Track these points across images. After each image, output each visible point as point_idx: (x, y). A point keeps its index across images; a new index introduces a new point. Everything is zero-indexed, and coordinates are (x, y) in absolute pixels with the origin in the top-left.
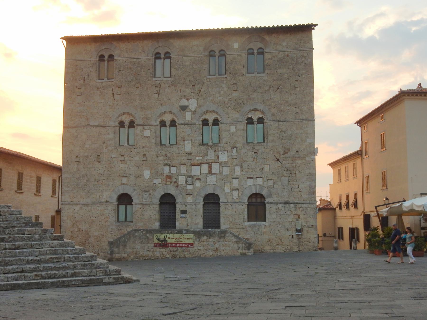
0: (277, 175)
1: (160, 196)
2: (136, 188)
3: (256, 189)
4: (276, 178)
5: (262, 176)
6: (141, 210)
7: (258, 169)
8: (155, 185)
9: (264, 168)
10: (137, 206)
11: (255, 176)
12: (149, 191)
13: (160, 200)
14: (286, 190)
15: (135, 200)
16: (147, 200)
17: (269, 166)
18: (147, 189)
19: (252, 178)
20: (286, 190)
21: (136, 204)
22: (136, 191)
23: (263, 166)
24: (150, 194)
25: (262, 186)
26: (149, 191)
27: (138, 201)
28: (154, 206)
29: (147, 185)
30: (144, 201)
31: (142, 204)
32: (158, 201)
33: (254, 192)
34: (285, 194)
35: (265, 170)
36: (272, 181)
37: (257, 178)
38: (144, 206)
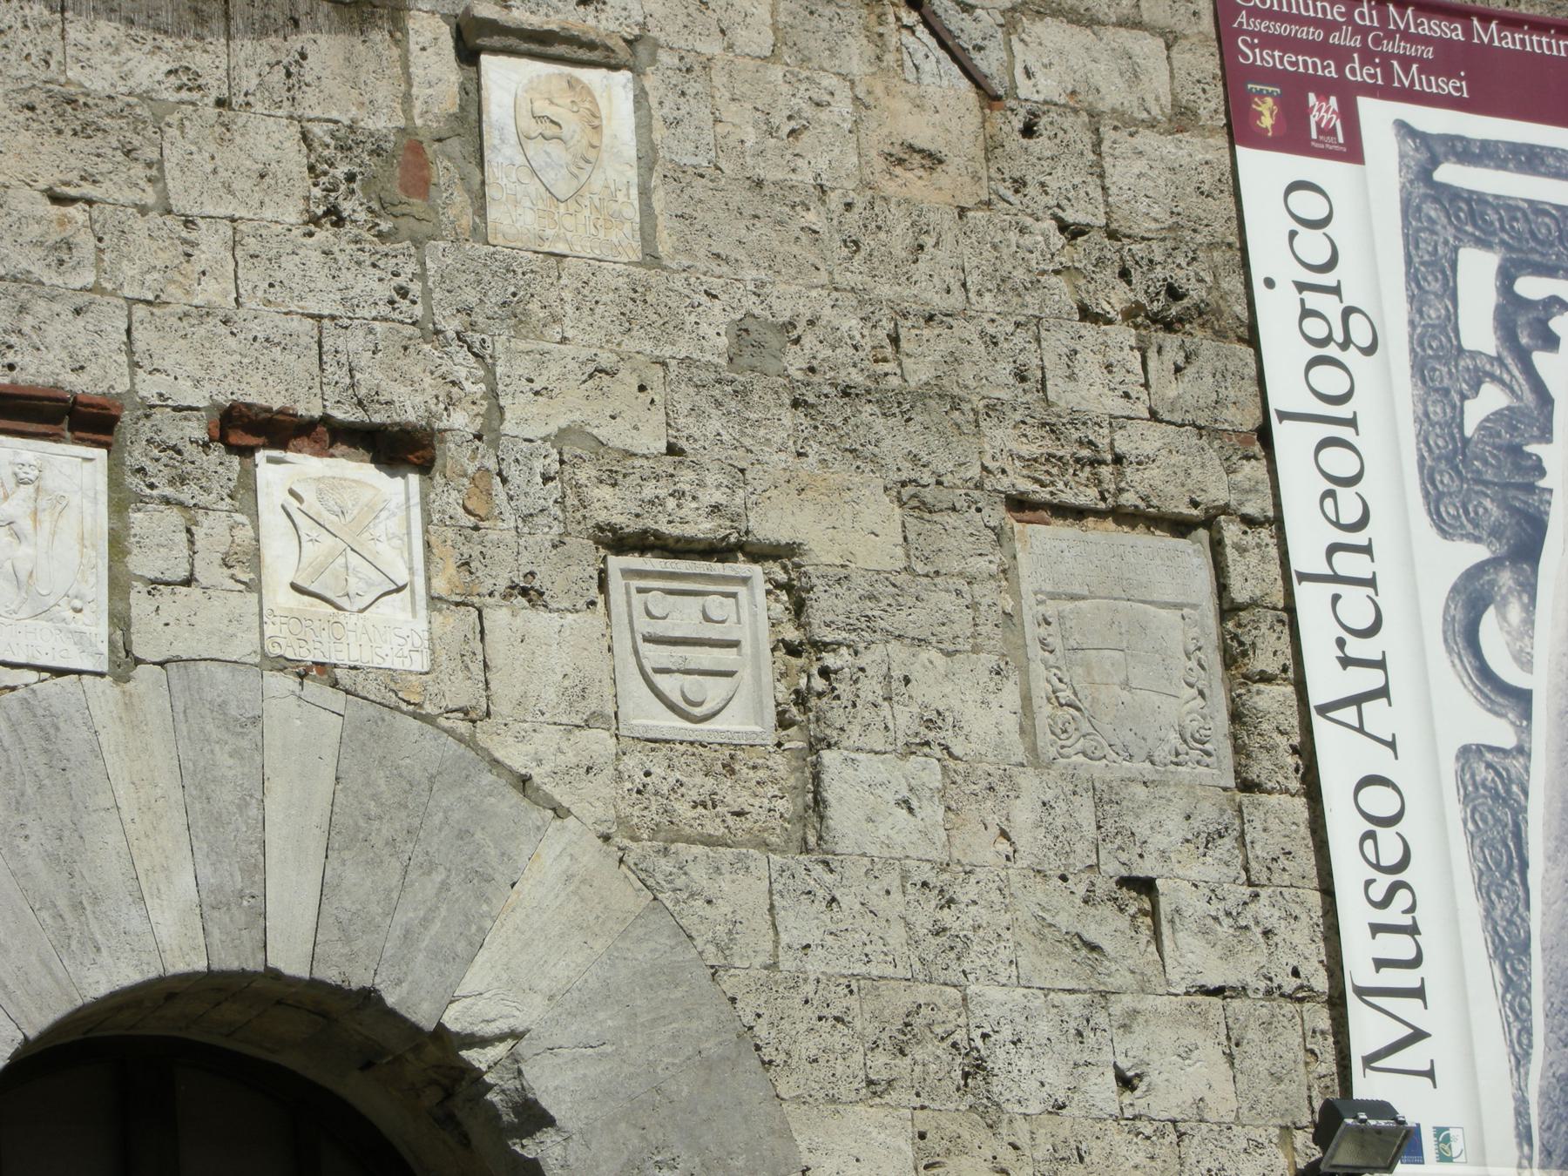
0: (896, 442)
3: (225, 823)
4: (848, 530)
5: (407, 405)
7: (269, 139)
9: (469, 118)
11: (188, 376)
14: (1194, 956)
17: (613, 91)
19: (89, 421)
20: (1194, 956)
23: (435, 65)
25: (427, 758)
33: (156, 933)
34: (1167, 1094)
35: (515, 215)
36: (748, 607)
37: (249, 429)
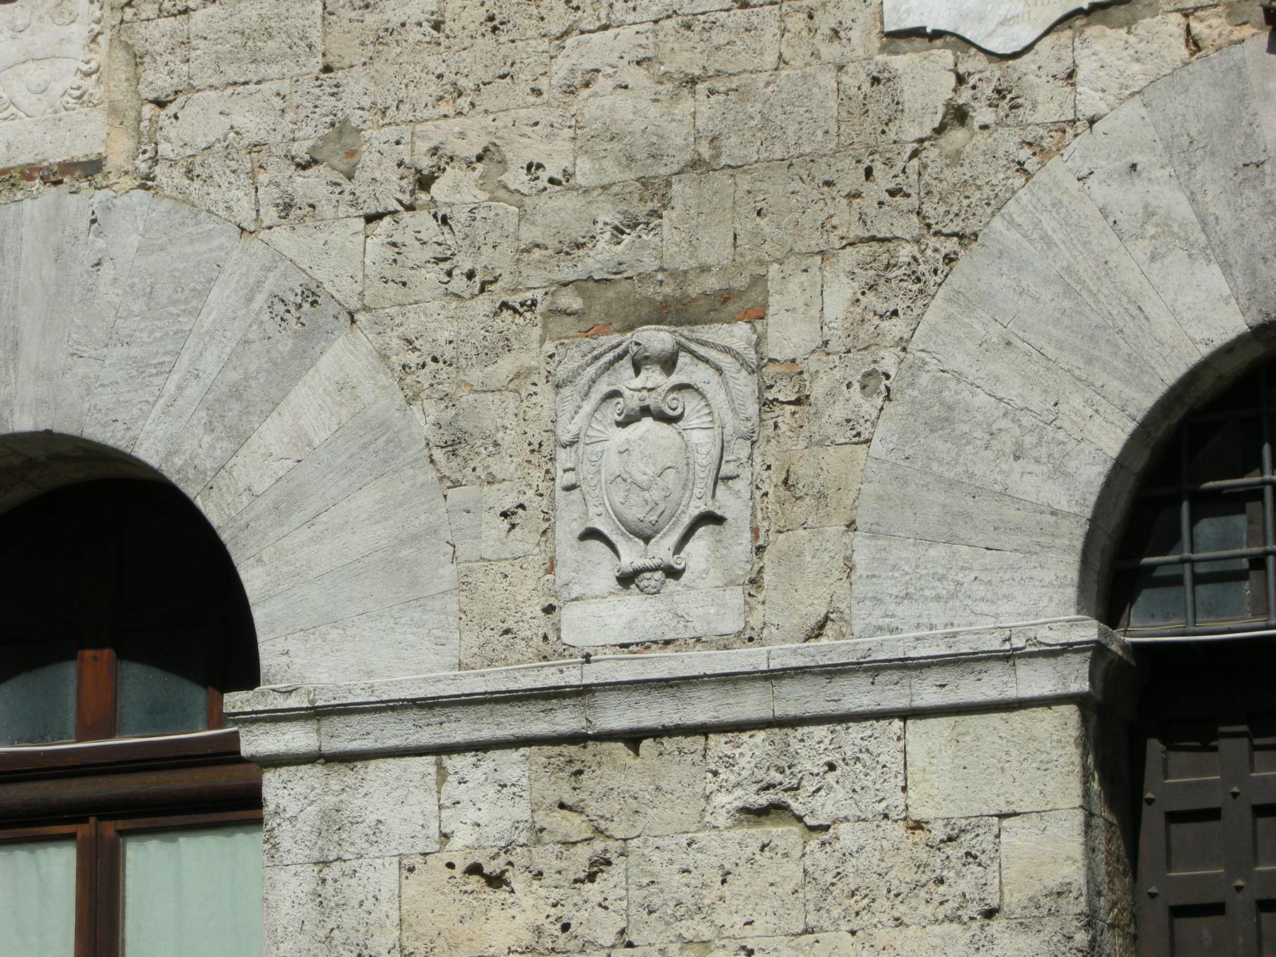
1: (1108, 437)
2: (340, 253)
6: (525, 908)
8: (925, 80)
10: (394, 799)
12: (741, 301)
13: (1123, 556)
15: (324, 625)
16: (706, 598)
18: (692, 241)
21: (350, 736)
22: (345, 356)
24: (781, 392)
26: (741, 301)
27: (411, 658)
28: (941, 769)
29: (680, 123)
30: (603, 620)
31: (570, 725)
32: (1042, 599)
38: (618, 772)
